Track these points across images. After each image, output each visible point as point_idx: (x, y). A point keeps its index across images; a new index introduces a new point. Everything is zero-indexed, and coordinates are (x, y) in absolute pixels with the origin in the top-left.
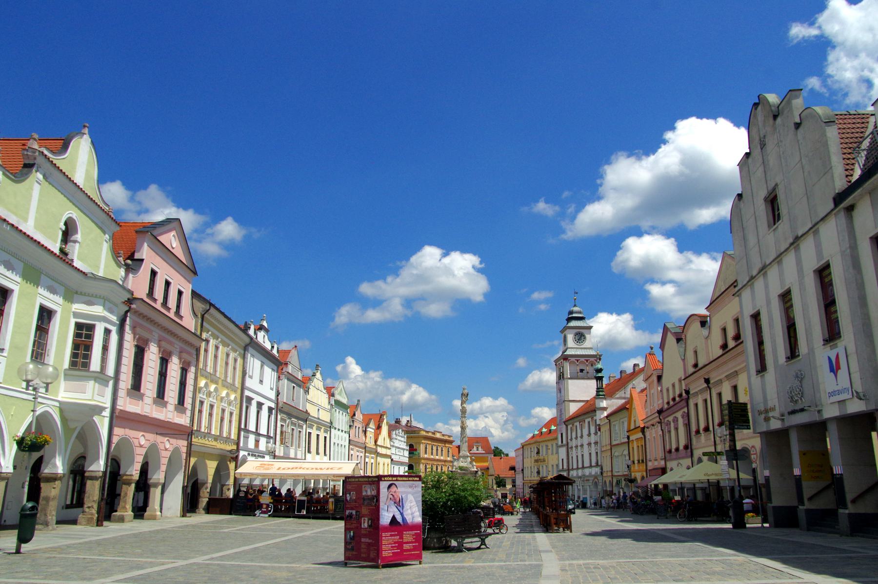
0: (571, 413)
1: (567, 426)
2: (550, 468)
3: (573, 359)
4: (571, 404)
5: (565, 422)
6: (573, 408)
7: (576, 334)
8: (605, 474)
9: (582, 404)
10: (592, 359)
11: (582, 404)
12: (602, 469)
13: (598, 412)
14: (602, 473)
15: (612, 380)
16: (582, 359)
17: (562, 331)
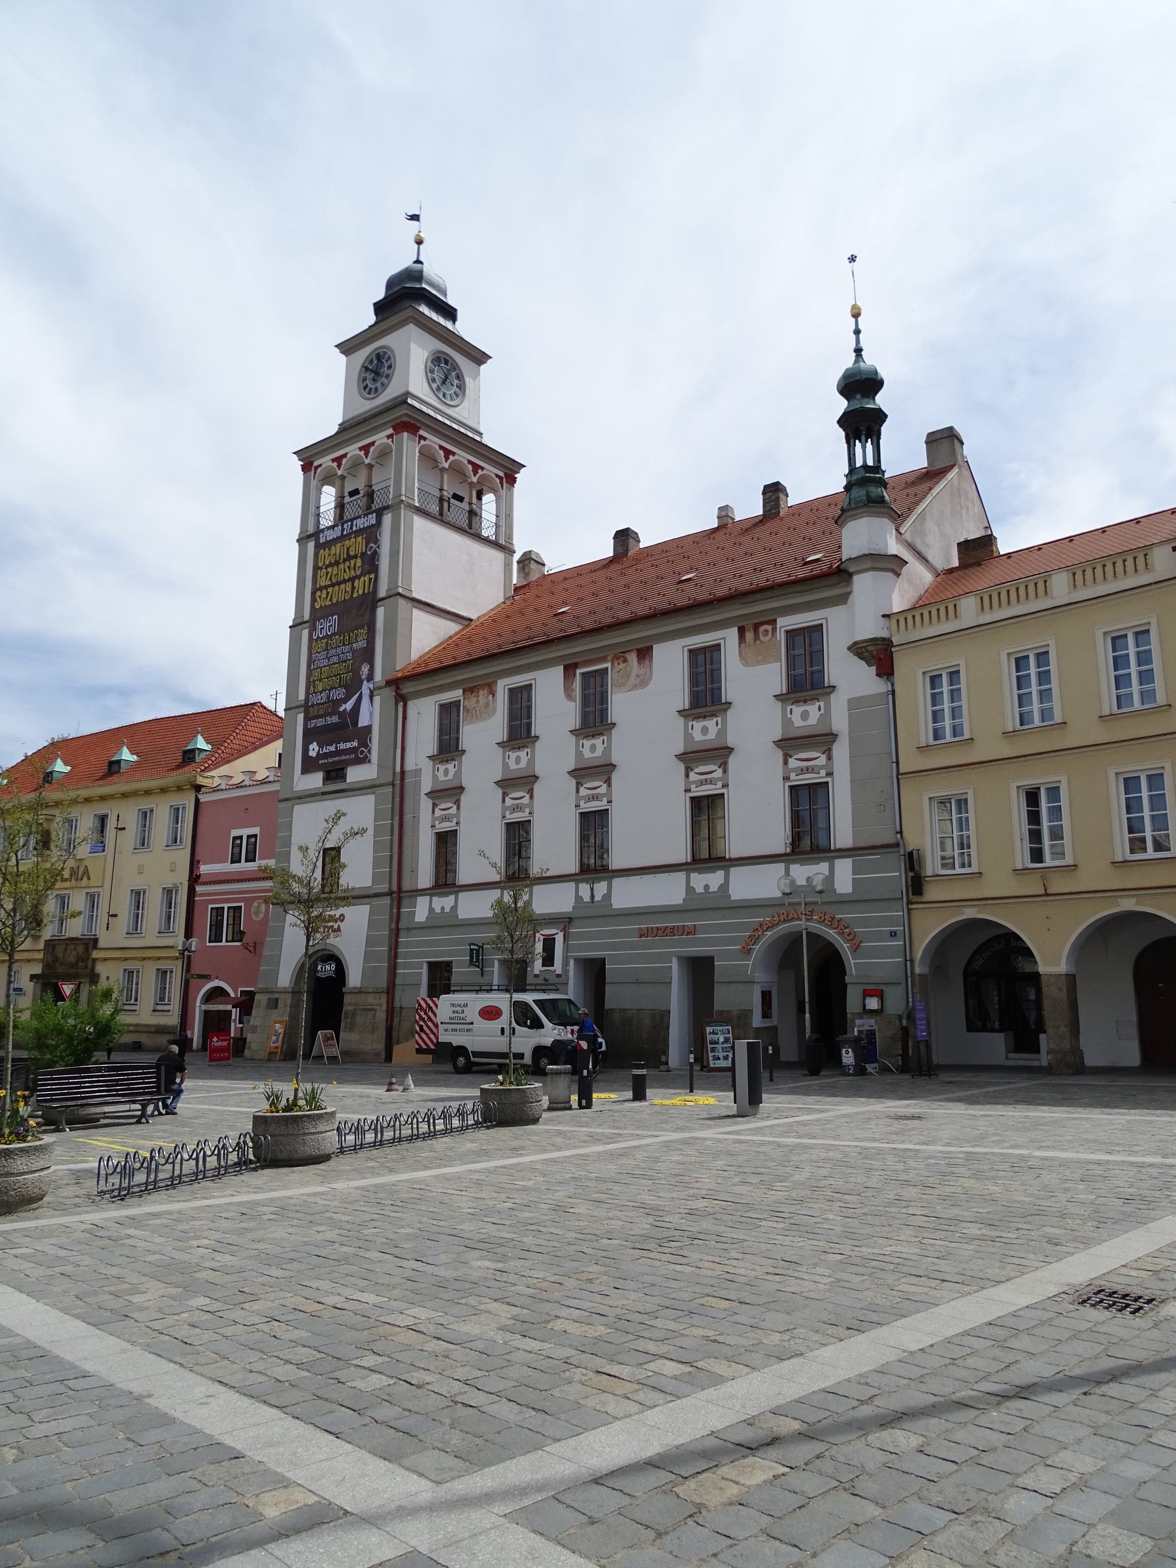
0: (415, 656)
1: (402, 699)
2: (124, 906)
3: (433, 441)
4: (418, 615)
5: (394, 683)
6: (424, 636)
7: (438, 359)
8: (933, 892)
9: (452, 628)
10: (490, 470)
11: (452, 628)
12: (913, 861)
13: (863, 583)
14: (917, 885)
15: (534, 576)
16: (462, 456)
17: (347, 348)
